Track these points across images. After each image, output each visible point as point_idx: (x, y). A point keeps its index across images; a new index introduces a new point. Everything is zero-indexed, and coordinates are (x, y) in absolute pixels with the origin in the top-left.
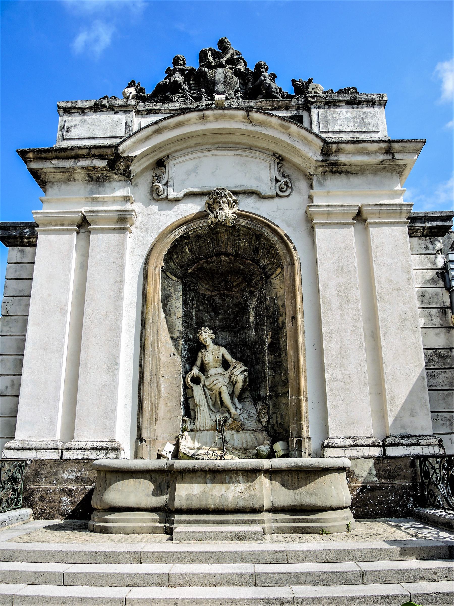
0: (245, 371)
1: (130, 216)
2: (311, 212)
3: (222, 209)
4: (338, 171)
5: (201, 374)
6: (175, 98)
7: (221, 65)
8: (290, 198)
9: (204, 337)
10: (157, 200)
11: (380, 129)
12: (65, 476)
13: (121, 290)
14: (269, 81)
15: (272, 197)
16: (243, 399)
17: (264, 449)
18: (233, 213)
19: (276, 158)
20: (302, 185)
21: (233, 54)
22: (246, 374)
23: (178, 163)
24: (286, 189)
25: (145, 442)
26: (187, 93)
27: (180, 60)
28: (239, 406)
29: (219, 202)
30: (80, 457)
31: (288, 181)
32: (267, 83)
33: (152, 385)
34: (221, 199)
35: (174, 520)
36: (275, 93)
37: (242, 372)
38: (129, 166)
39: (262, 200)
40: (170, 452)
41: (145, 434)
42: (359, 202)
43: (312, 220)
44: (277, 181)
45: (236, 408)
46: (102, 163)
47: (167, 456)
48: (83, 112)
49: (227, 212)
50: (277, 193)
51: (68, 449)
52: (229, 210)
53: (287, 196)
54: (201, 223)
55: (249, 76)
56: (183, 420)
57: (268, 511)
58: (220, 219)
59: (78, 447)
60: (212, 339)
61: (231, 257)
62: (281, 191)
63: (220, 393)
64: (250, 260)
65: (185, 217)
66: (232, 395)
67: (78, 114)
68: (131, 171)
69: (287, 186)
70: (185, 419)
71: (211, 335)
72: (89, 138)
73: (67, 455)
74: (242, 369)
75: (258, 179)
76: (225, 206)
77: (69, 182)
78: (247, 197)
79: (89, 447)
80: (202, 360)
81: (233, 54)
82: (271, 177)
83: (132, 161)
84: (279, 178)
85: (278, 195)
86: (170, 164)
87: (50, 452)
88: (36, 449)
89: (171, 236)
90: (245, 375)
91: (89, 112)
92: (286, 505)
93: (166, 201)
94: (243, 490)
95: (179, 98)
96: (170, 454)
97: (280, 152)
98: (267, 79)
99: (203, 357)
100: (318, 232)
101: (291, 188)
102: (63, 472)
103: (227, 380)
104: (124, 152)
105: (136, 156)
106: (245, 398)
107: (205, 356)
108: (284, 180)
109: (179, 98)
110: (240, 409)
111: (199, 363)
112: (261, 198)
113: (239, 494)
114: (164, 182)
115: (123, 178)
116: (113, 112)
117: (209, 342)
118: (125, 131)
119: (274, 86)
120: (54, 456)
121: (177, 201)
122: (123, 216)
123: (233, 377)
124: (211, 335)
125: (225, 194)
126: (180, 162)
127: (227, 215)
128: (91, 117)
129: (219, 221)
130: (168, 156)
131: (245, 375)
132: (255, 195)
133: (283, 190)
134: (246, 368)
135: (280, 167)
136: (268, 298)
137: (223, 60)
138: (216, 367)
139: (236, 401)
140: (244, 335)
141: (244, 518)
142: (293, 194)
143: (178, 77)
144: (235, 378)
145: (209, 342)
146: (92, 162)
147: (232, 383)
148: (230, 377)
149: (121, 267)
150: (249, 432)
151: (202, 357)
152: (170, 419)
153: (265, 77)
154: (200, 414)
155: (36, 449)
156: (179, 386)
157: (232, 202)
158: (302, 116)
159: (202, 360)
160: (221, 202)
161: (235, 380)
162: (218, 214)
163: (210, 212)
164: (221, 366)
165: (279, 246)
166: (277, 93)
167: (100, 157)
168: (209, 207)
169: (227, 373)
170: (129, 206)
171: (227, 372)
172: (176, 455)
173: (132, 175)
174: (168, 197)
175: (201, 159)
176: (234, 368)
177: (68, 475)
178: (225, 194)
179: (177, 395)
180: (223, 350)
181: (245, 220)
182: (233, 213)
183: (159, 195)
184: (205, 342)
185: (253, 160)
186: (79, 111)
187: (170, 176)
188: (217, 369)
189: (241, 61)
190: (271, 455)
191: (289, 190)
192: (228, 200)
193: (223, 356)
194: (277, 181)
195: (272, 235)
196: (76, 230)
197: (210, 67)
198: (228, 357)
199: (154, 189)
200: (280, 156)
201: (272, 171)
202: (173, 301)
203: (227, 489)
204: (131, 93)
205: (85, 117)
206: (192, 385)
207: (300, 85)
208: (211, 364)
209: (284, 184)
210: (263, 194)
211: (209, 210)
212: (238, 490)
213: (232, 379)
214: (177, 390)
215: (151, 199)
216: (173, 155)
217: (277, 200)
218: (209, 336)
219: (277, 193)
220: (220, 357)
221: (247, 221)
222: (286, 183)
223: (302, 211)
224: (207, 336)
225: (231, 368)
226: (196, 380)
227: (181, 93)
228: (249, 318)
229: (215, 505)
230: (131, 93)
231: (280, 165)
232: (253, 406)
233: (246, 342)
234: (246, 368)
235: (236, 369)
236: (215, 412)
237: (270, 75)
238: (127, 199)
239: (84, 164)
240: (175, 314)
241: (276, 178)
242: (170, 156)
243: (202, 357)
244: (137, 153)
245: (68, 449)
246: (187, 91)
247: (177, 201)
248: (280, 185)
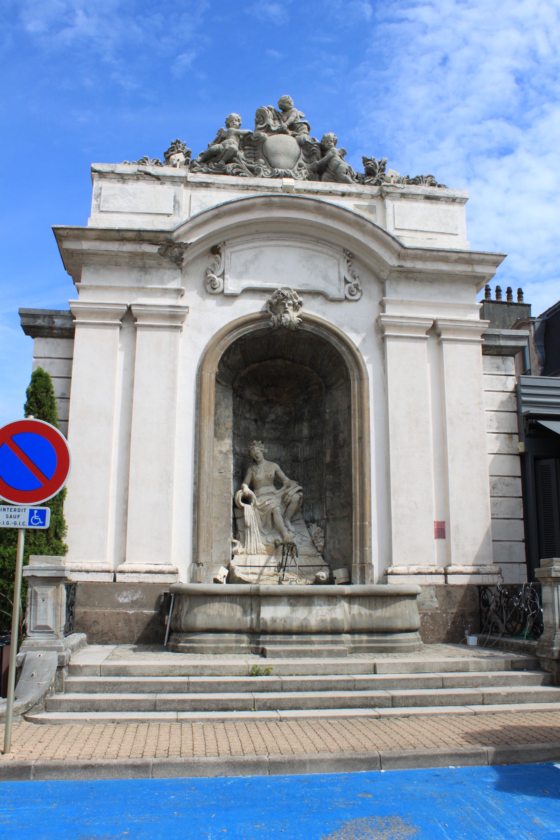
0: (299, 491)
1: (183, 313)
2: (383, 322)
3: (287, 312)
4: (413, 278)
5: (251, 492)
6: (229, 168)
7: (281, 131)
8: (359, 302)
9: (257, 451)
10: (211, 294)
11: (458, 232)
12: (121, 600)
13: (173, 398)
14: (338, 158)
15: (340, 301)
16: (294, 521)
17: (323, 575)
18: (298, 317)
19: (347, 255)
20: (374, 289)
21: (297, 117)
22: (301, 494)
23: (236, 252)
24: (356, 294)
25: (202, 565)
26: (243, 162)
27: (236, 120)
28: (292, 528)
29: (284, 304)
30: (136, 580)
31: (359, 283)
32: (335, 160)
33: (208, 506)
34: (286, 301)
35: (259, 641)
36: (344, 174)
37: (297, 492)
38: (181, 254)
39: (329, 302)
40: (224, 576)
41: (202, 559)
42: (435, 316)
43: (383, 332)
44: (346, 282)
45: (289, 530)
46: (154, 249)
47: (222, 580)
48: (122, 178)
49: (292, 316)
50: (346, 297)
51: (121, 572)
52: (294, 313)
53: (356, 301)
54: (262, 325)
55: (314, 148)
56: (232, 543)
57: (348, 632)
58: (284, 324)
59: (132, 570)
60: (264, 454)
61: (288, 362)
62: (350, 294)
63: (272, 514)
64: (309, 367)
65: (243, 317)
66: (284, 516)
67: (116, 180)
68: (183, 259)
69: (357, 289)
70: (235, 541)
71: (263, 449)
72: (131, 213)
73: (120, 578)
74: (297, 489)
75: (326, 278)
76: (290, 309)
77: (110, 267)
78: (313, 298)
79: (145, 570)
80: (252, 477)
81: (297, 117)
82: (340, 278)
83: (186, 248)
84: (349, 279)
85: (346, 298)
86: (226, 252)
87: (101, 575)
88: (88, 572)
89: (228, 338)
90: (300, 495)
91: (129, 179)
92: (364, 627)
93: (221, 296)
94: (325, 613)
95: (234, 168)
96: (225, 579)
97: (351, 250)
98: (337, 155)
99: (254, 474)
100: (390, 344)
101: (361, 291)
102: (118, 596)
103: (279, 501)
104: (178, 237)
105: (191, 243)
106: (297, 520)
107: (256, 472)
108: (355, 282)
109: (234, 168)
110: (293, 532)
111: (248, 479)
112: (328, 300)
113: (321, 617)
114: (220, 273)
115: (174, 265)
116: (159, 182)
117: (261, 455)
118: (174, 207)
119: (344, 165)
120: (108, 578)
121: (234, 296)
122: (175, 313)
123: (287, 497)
124: (263, 449)
125: (291, 296)
126: (239, 251)
127: (292, 319)
128: (132, 186)
129: (283, 325)
130: (224, 243)
131: (300, 495)
132: (321, 297)
133: (353, 293)
134: (301, 488)
135: (350, 266)
136: (328, 411)
137: (285, 125)
138: (267, 486)
139: (289, 522)
140: (295, 449)
141: (325, 639)
142: (364, 299)
143: (233, 143)
144: (290, 498)
145: (261, 455)
146: (141, 248)
147: (286, 504)
148: (283, 497)
149: (173, 373)
150: (304, 556)
151: (252, 474)
152: (219, 541)
153: (334, 153)
154: (251, 536)
155: (88, 572)
156: (228, 505)
157: (297, 304)
158: (375, 207)
159: (252, 477)
160: (287, 304)
161: (289, 501)
162: (283, 318)
163: (272, 314)
164: (273, 484)
165: (348, 358)
166: (346, 174)
167: (152, 242)
168: (271, 308)
169: (280, 492)
170: (180, 302)
171: (279, 491)
172: (231, 578)
173: (184, 264)
174: (225, 292)
175: (261, 249)
176: (288, 487)
177: (123, 598)
178: (291, 296)
179: (227, 515)
180: (275, 467)
181: (310, 325)
182: (298, 317)
183: (215, 289)
184: (257, 458)
185: (321, 254)
186: (118, 177)
187: (227, 267)
188: (269, 487)
189: (305, 126)
190: (331, 581)
191: (359, 295)
192: (293, 302)
193: (276, 474)
194: (346, 282)
195: (340, 345)
196: (119, 325)
197: (268, 129)
198: (282, 474)
199: (209, 281)
200: (350, 253)
201: (342, 270)
202: (222, 409)
203: (310, 612)
204: (178, 160)
205: (125, 186)
206: (242, 504)
207: (372, 165)
208: (262, 482)
209: (354, 287)
210: (331, 297)
211: (271, 311)
212: (320, 613)
213: (285, 499)
214: (226, 510)
215: (204, 292)
216: (230, 242)
217: (345, 305)
218: (261, 451)
219: (346, 297)
220: (273, 474)
221: (312, 327)
222: (356, 286)
223: (372, 320)
224: (259, 451)
225: (284, 488)
226: (247, 500)
227: (238, 163)
228: (301, 430)
229: (323, 621)
230: (178, 160)
231: (349, 264)
232: (306, 529)
233: (297, 457)
234: (301, 488)
235: (290, 489)
236: (266, 534)
237: (339, 151)
238: (179, 292)
239: (131, 249)
240: (225, 424)
241: (345, 279)
242: (226, 243)
243: (252, 474)
244: (193, 240)
245: (121, 572)
246: (243, 159)
247: (234, 296)
248: (350, 287)
